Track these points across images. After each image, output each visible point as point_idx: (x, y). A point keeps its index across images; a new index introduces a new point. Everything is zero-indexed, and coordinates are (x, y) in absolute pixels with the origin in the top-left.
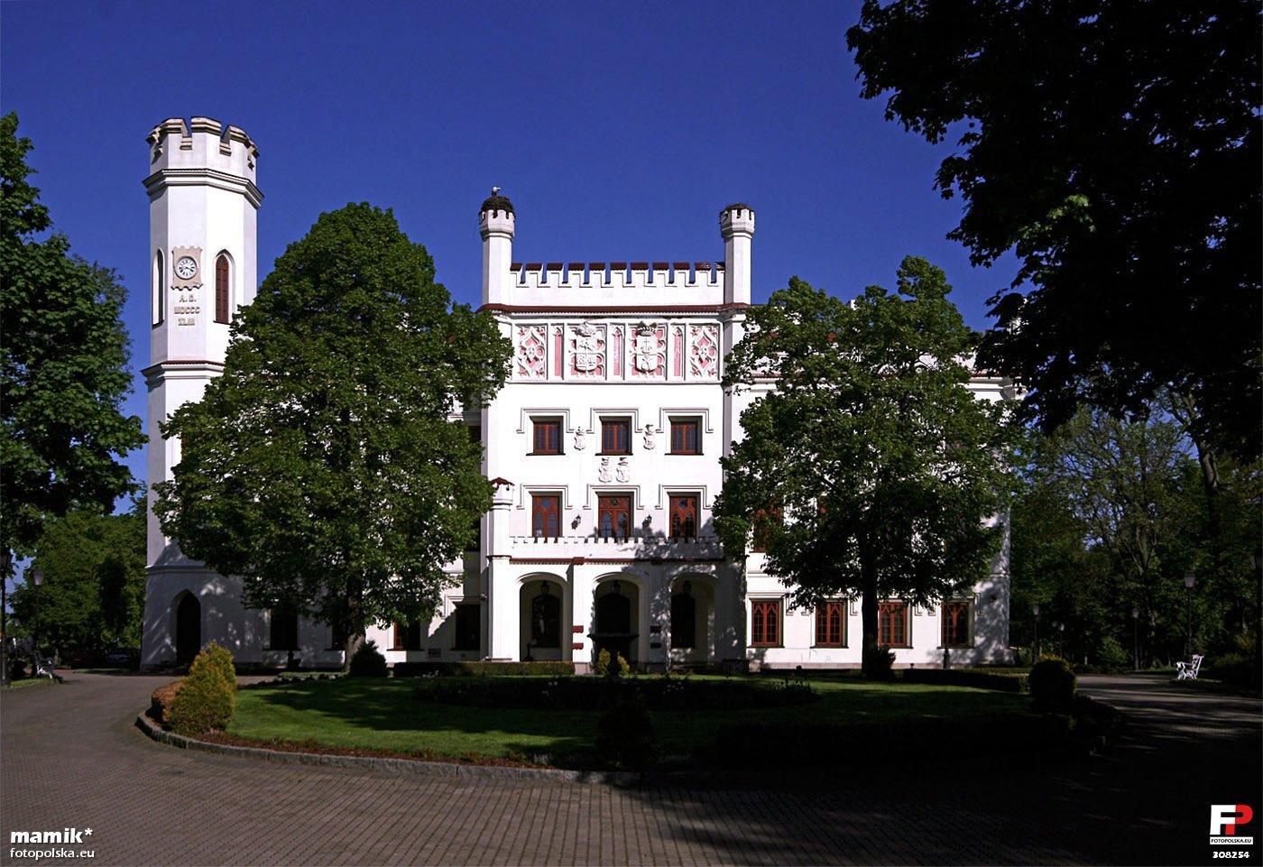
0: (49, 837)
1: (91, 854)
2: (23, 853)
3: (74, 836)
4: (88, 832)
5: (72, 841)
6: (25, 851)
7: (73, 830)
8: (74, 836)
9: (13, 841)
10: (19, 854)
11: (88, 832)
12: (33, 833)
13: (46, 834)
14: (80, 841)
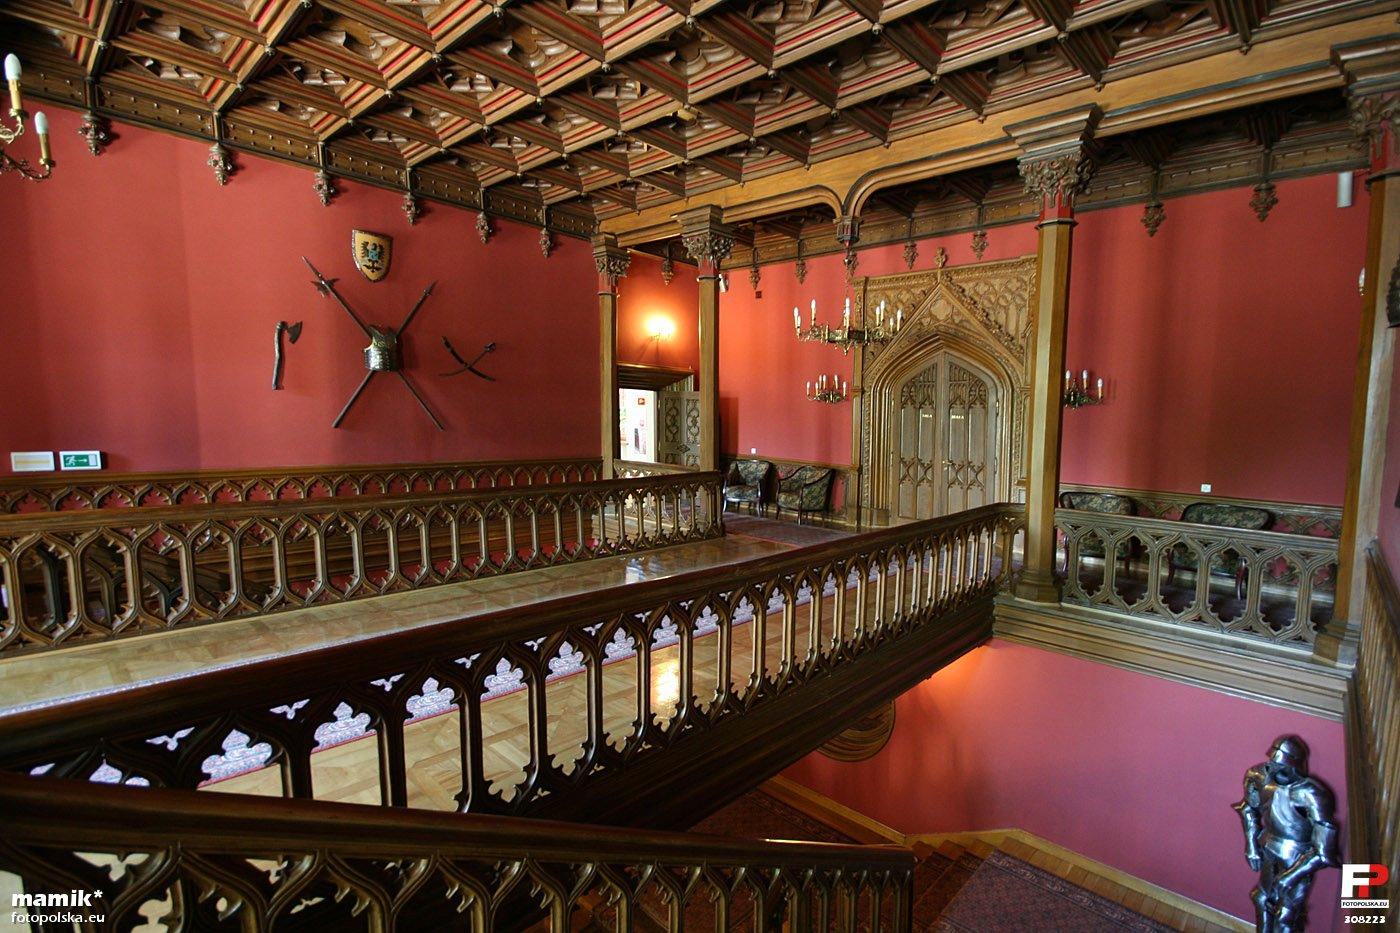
0: (55, 900)
5: (80, 904)
13: (51, 897)
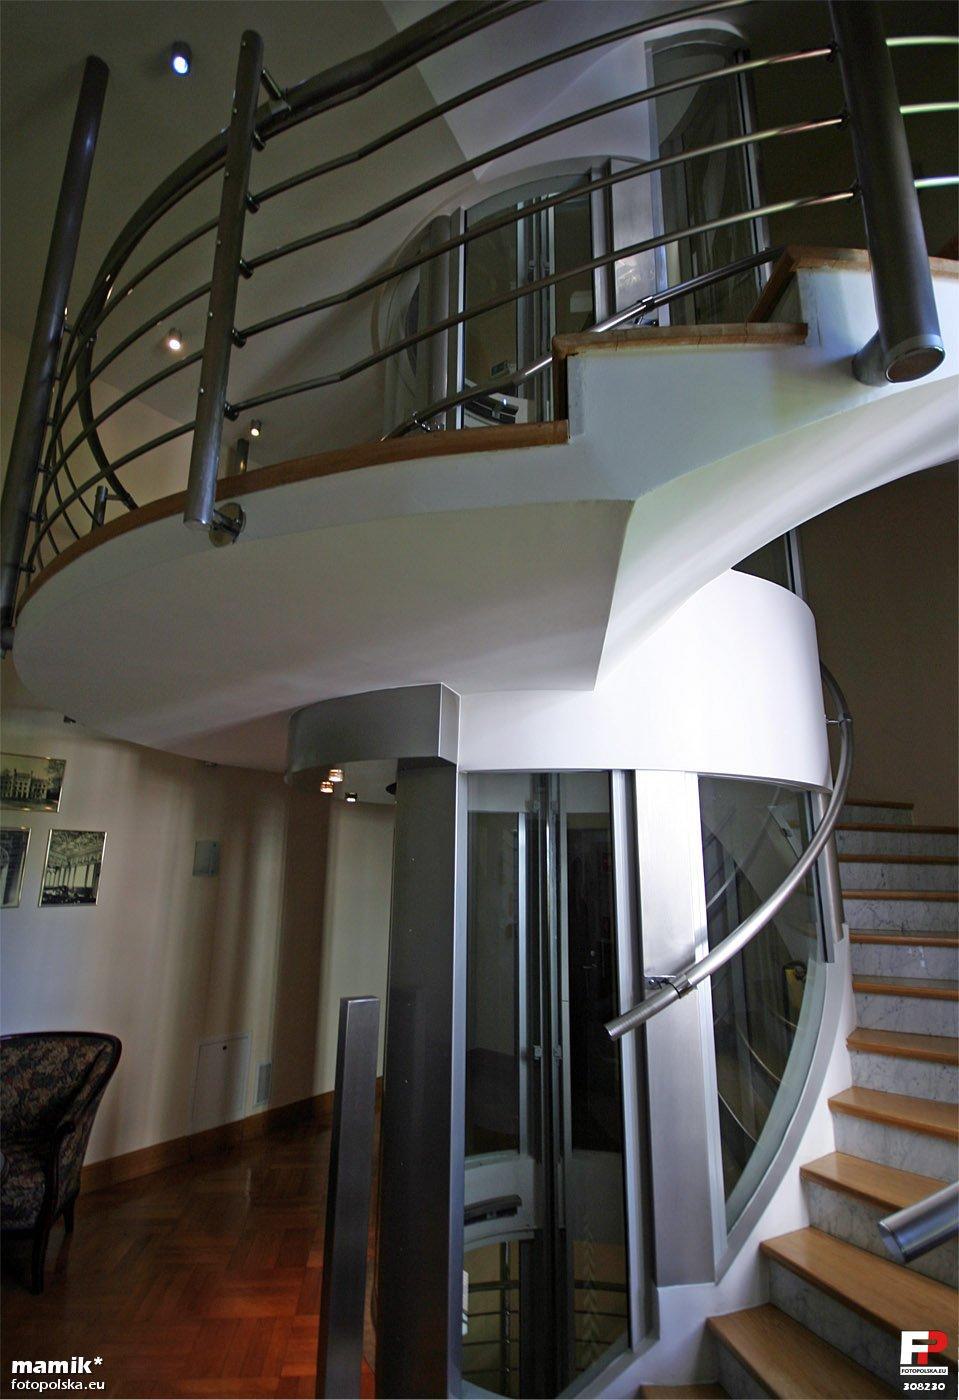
0: (55, 1367)
1: (100, 1385)
2: (26, 1385)
3: (82, 1366)
4: (98, 1361)
6: (28, 1382)
7: (81, 1359)
8: (82, 1366)
9: (14, 1371)
10: (21, 1385)
11: (98, 1361)
12: (37, 1363)
13: (51, 1364)
14: (88, 1371)
